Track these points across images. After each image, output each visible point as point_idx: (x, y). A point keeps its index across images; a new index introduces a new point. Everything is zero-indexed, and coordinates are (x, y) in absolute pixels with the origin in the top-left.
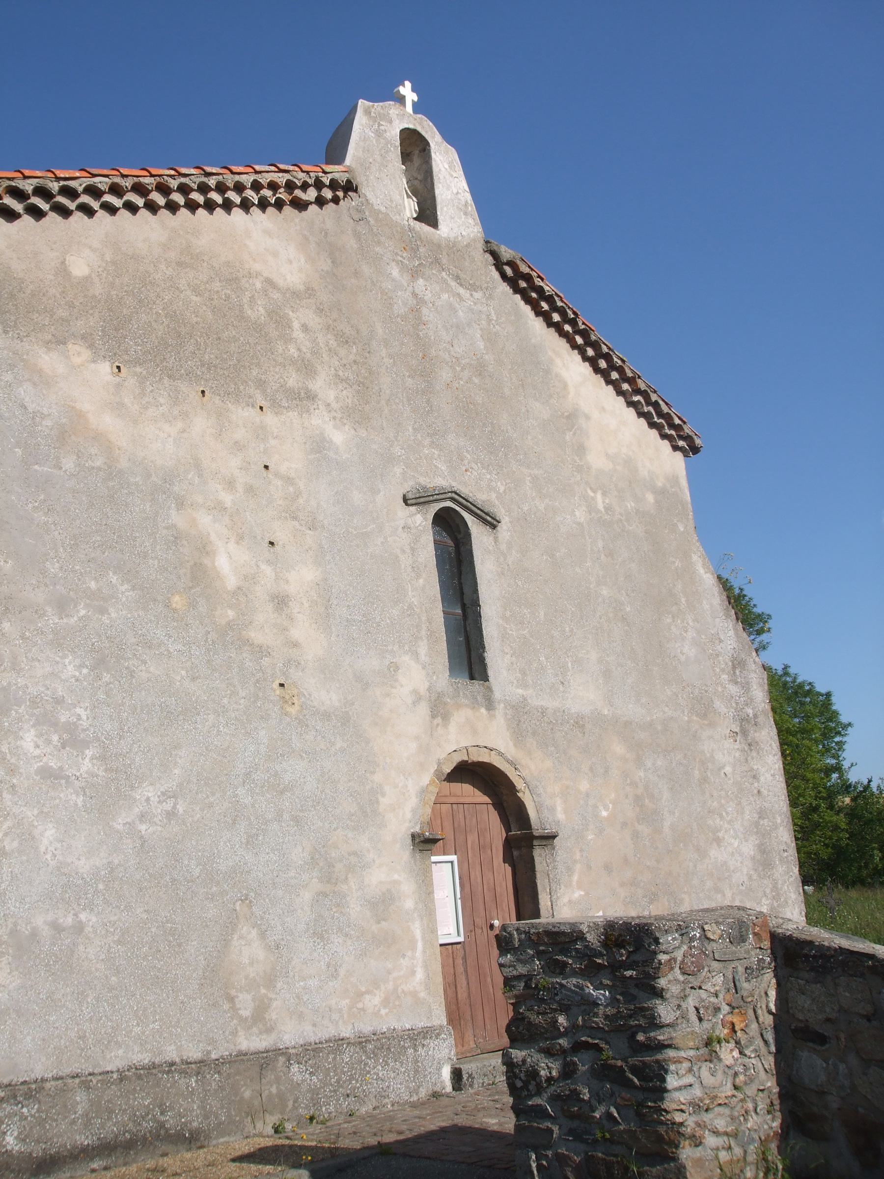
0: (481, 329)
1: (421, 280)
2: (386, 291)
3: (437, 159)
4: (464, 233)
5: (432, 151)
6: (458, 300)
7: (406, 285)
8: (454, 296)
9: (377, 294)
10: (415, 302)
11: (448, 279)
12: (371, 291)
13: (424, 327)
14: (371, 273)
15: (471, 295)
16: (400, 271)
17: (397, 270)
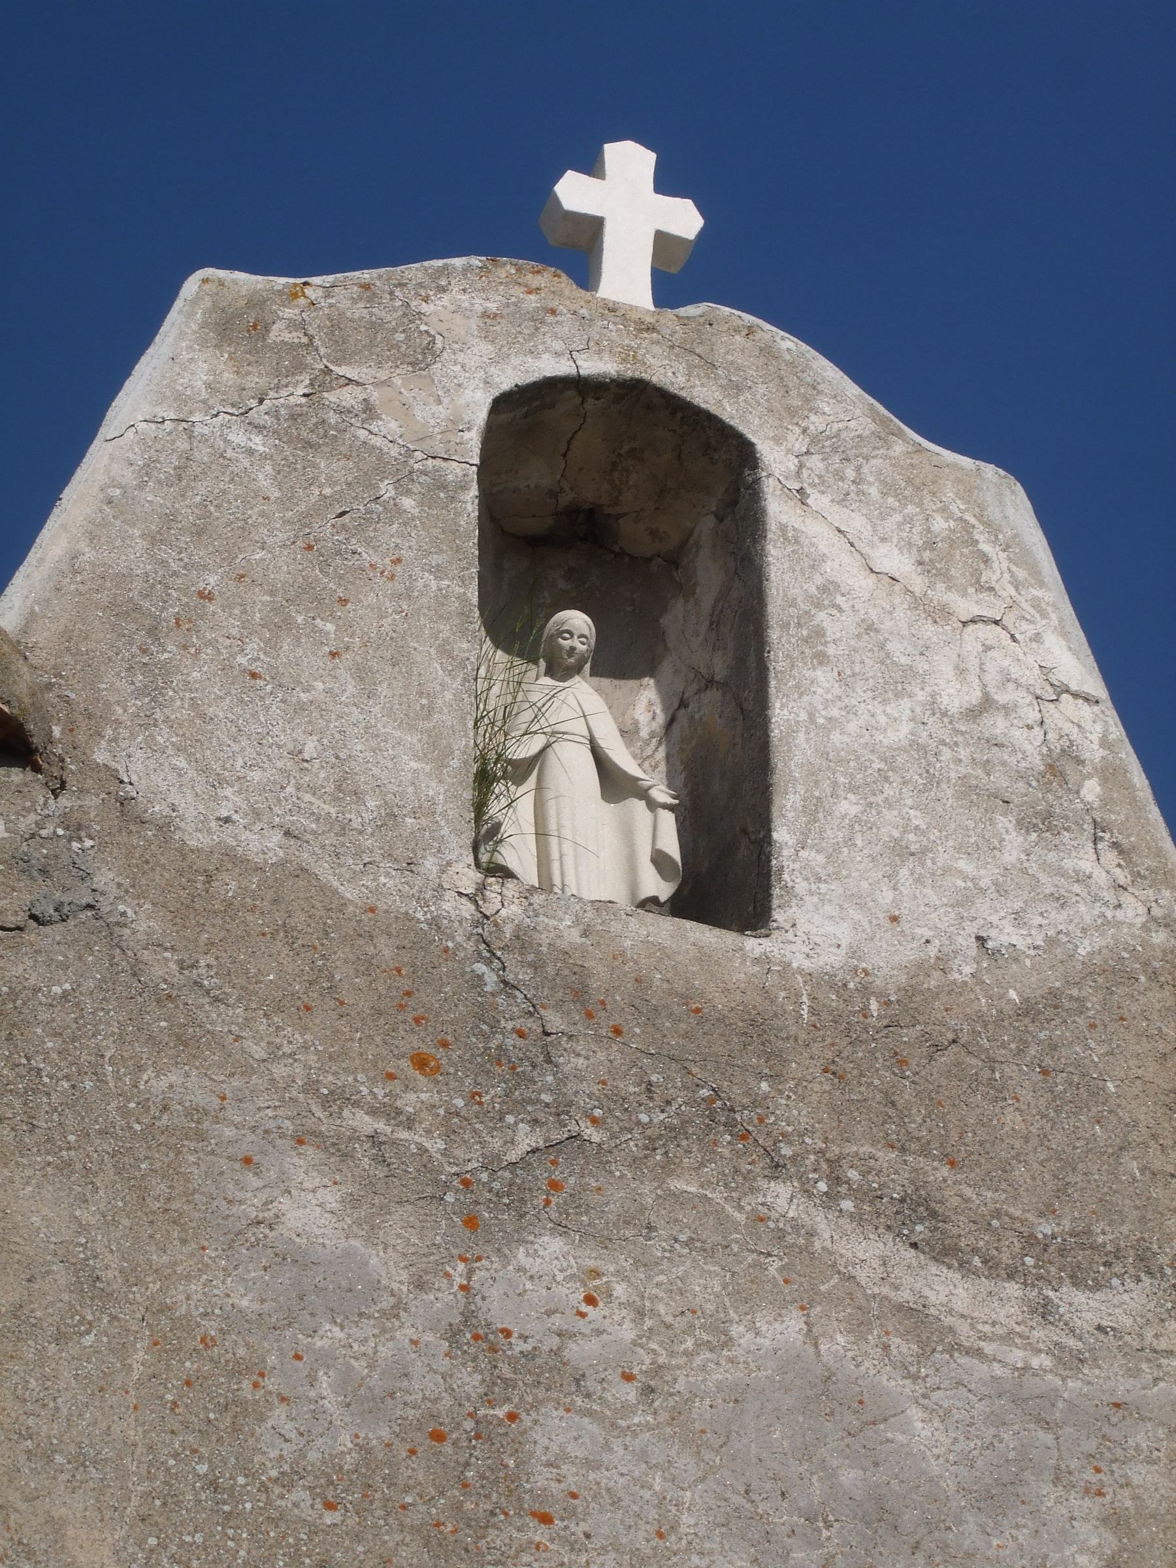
0: (1114, 1520)
1: (553, 1245)
2: (211, 1327)
3: (813, 529)
4: (1005, 935)
5: (769, 487)
6: (902, 1347)
7: (400, 1280)
8: (859, 1327)
9: (123, 1350)
10: (470, 1381)
11: (822, 1222)
12: (60, 1338)
13: (539, 1533)
14: (83, 1228)
15: (1044, 1311)
16: (352, 1201)
17: (331, 1198)
